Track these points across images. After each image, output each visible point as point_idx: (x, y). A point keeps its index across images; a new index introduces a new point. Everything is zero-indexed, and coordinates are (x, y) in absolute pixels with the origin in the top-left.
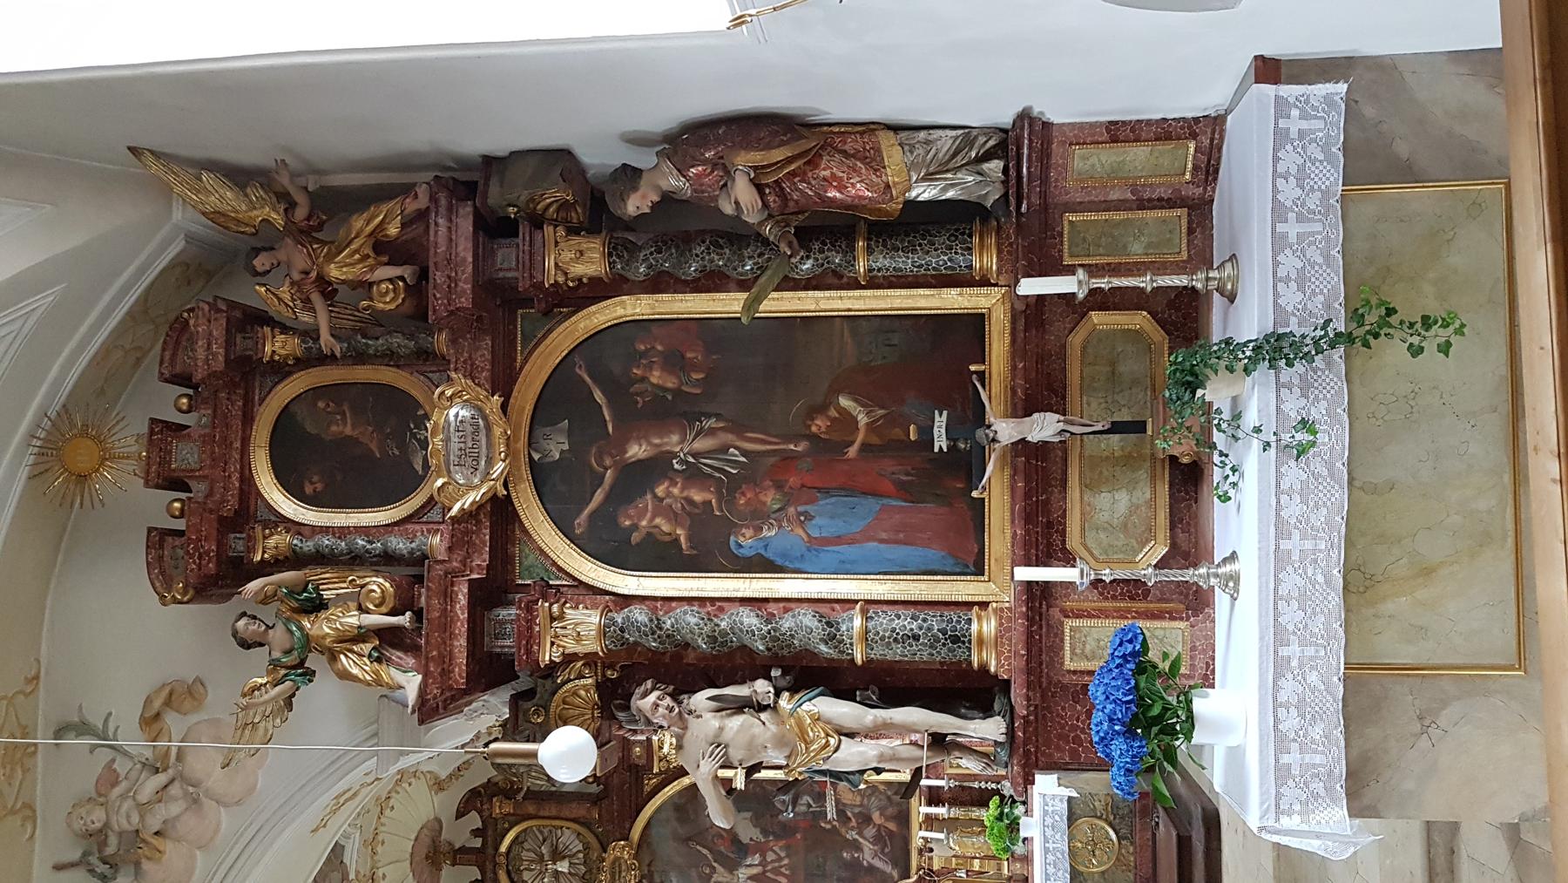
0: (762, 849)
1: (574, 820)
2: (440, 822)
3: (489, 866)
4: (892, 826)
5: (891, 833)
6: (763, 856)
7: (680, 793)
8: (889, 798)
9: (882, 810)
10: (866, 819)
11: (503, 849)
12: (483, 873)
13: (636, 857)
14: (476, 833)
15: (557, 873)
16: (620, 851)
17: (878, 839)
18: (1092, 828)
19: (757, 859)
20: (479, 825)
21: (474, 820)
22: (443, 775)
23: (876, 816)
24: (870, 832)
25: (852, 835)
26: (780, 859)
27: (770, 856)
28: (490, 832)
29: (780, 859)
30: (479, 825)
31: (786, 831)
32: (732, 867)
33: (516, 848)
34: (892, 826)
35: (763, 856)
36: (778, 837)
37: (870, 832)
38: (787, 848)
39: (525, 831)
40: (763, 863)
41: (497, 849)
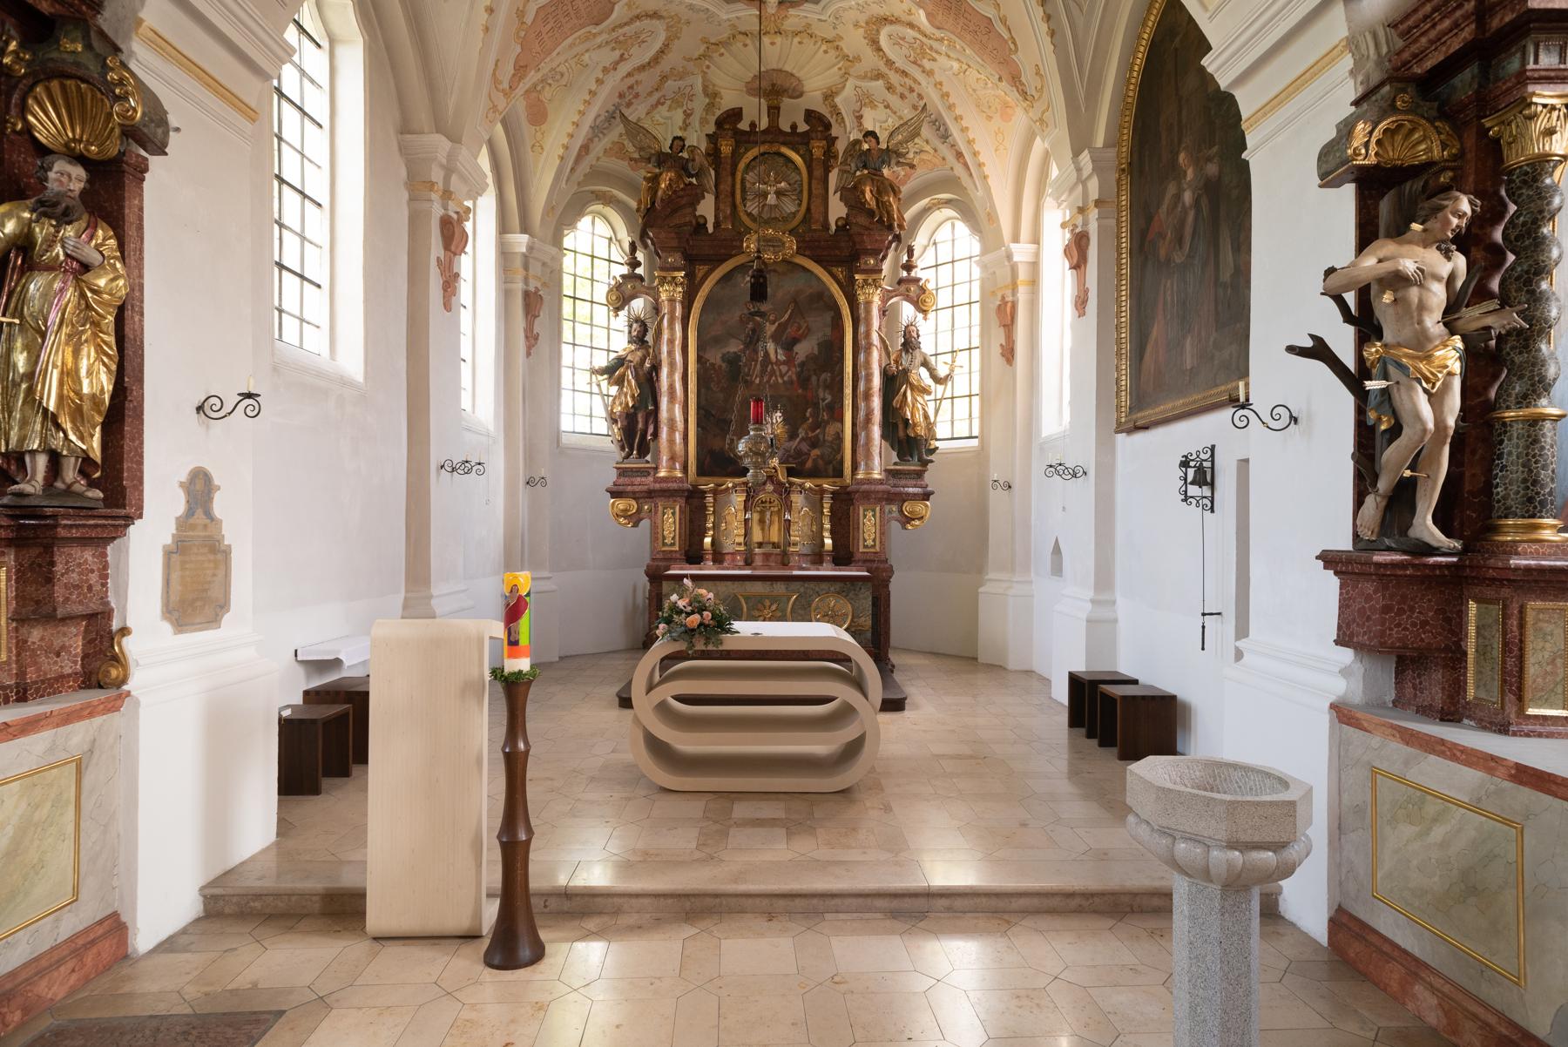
0: (789, 361)
1: (808, 209)
2: (801, 95)
3: (769, 138)
4: (809, 464)
5: (803, 463)
6: (784, 363)
7: (832, 296)
8: (830, 462)
9: (822, 457)
10: (814, 444)
11: (785, 150)
12: (765, 132)
13: (784, 260)
14: (794, 127)
15: (765, 195)
16: (791, 244)
17: (799, 453)
18: (846, 615)
19: (782, 357)
20: (799, 130)
21: (803, 127)
22: (838, 100)
23: (816, 452)
24: (805, 447)
25: (802, 433)
26: (782, 376)
27: (784, 368)
28: (797, 140)
29: (782, 376)
30: (799, 130)
31: (804, 381)
32: (776, 338)
33: (781, 160)
34: (809, 464)
35: (784, 363)
36: (799, 375)
37: (805, 447)
38: (791, 382)
39: (797, 168)
40: (778, 363)
41: (784, 144)
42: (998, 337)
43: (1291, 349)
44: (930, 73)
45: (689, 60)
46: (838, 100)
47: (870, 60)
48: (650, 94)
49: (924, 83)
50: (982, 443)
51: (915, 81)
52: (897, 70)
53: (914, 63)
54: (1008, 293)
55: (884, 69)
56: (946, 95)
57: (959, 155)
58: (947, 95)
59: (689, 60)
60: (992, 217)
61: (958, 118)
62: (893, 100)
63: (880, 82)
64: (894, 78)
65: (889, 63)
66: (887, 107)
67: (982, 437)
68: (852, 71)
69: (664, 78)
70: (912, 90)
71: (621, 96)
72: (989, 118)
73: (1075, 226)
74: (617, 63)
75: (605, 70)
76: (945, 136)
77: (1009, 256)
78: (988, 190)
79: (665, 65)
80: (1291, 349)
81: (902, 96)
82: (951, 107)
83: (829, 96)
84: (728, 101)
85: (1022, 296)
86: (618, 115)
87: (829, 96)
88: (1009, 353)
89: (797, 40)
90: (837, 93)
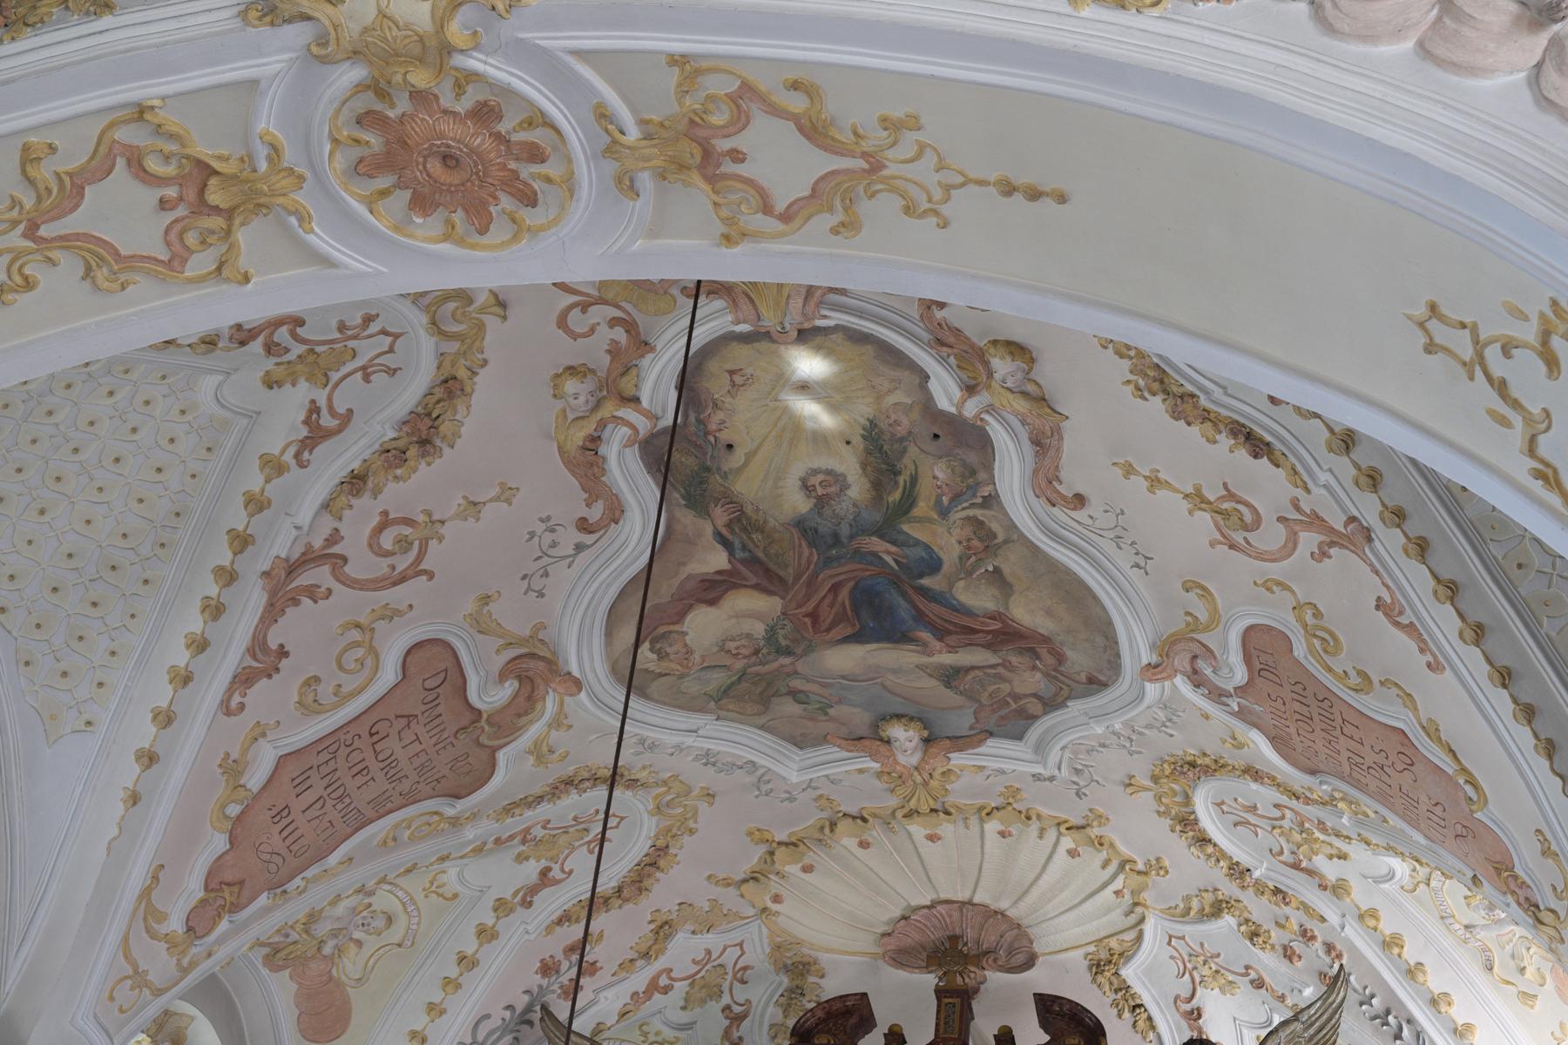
2: (1030, 962)
22: (1129, 972)
44: (1338, 889)
45: (727, 883)
46: (1129, 972)
47: (1188, 871)
48: (627, 966)
49: (1333, 918)
51: (1305, 908)
52: (1260, 887)
53: (1296, 866)
55: (1229, 889)
56: (1391, 944)
59: (727, 883)
62: (1268, 962)
63: (1228, 920)
64: (1260, 909)
65: (1238, 872)
66: (1259, 984)
68: (1146, 896)
69: (663, 930)
70: (1307, 936)
71: (547, 969)
72: (1527, 997)
74: (533, 890)
75: (502, 907)
79: (664, 894)
81: (1289, 954)
83: (1104, 965)
84: (834, 985)
86: (536, 1016)
87: (1104, 965)
89: (992, 826)
90: (1126, 955)
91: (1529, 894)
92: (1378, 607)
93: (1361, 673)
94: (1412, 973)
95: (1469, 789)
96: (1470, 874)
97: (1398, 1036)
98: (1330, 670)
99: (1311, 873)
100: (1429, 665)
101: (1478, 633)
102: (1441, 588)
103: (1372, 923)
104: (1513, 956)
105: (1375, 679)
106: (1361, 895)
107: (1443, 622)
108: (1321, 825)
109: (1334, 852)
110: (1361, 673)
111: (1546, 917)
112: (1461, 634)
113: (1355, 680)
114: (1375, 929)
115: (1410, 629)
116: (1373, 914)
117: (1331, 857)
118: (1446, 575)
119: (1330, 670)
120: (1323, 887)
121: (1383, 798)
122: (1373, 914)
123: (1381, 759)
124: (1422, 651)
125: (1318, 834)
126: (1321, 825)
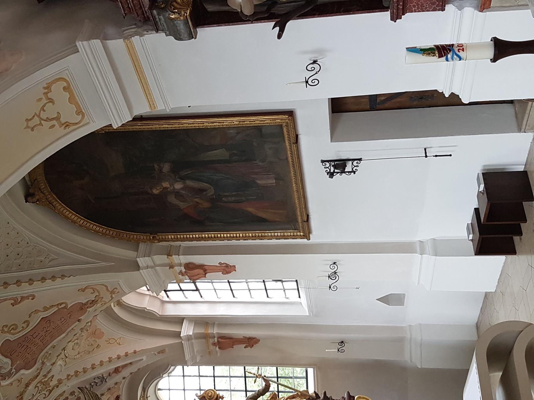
42: (240, 349)
43: (279, 36)
44: (60, 381)
49: (65, 388)
50: (310, 366)
51: (61, 395)
54: (211, 341)
57: (117, 370)
58: (76, 372)
60: (161, 351)
61: (93, 367)
67: (306, 365)
73: (181, 273)
76: (103, 379)
77: (189, 338)
78: (144, 352)
80: (279, 36)
82: (85, 371)
85: (215, 331)
88: (251, 342)
91: (91, 301)
92: (13, 306)
93: (24, 323)
94: (85, 371)
95: (63, 306)
96: (77, 323)
97: (96, 384)
98: (20, 332)
99: (53, 389)
100: (32, 299)
101: (31, 281)
102: (18, 284)
103: (70, 377)
104: (88, 346)
105: (28, 319)
106: (64, 377)
107: (26, 289)
108: (45, 376)
109: (50, 380)
110: (24, 323)
111: (97, 299)
112: (30, 284)
113: (25, 325)
114: (72, 376)
115: (23, 298)
116: (68, 375)
117: (52, 380)
118: (15, 282)
119: (20, 332)
120: (57, 387)
121: (53, 338)
122: (68, 375)
123: (45, 331)
124: (28, 299)
125: (46, 380)
126: (45, 376)
